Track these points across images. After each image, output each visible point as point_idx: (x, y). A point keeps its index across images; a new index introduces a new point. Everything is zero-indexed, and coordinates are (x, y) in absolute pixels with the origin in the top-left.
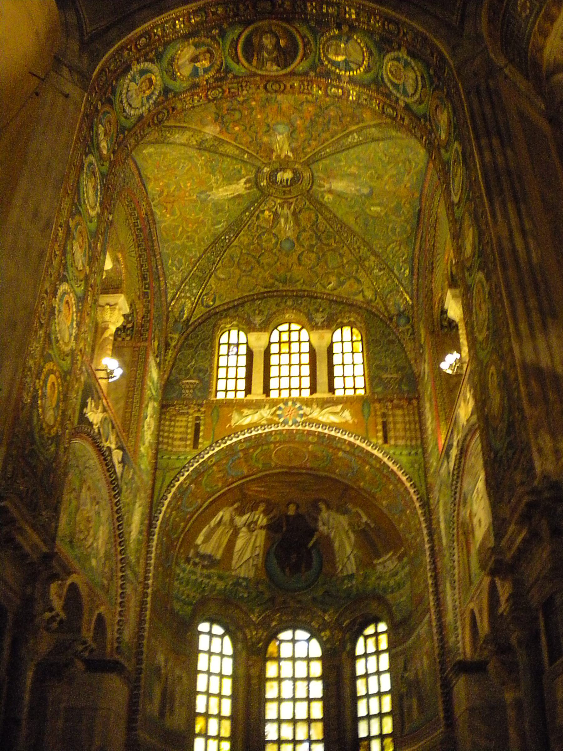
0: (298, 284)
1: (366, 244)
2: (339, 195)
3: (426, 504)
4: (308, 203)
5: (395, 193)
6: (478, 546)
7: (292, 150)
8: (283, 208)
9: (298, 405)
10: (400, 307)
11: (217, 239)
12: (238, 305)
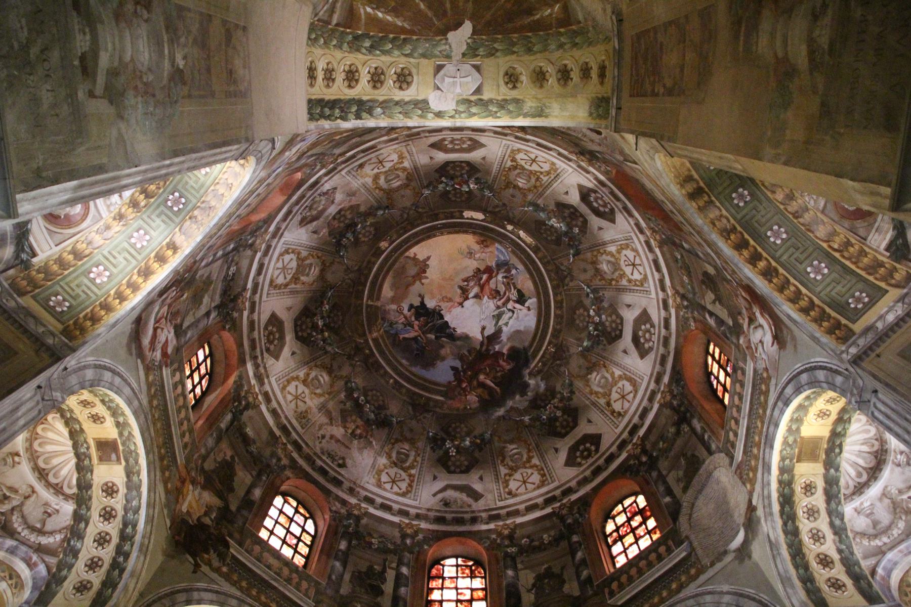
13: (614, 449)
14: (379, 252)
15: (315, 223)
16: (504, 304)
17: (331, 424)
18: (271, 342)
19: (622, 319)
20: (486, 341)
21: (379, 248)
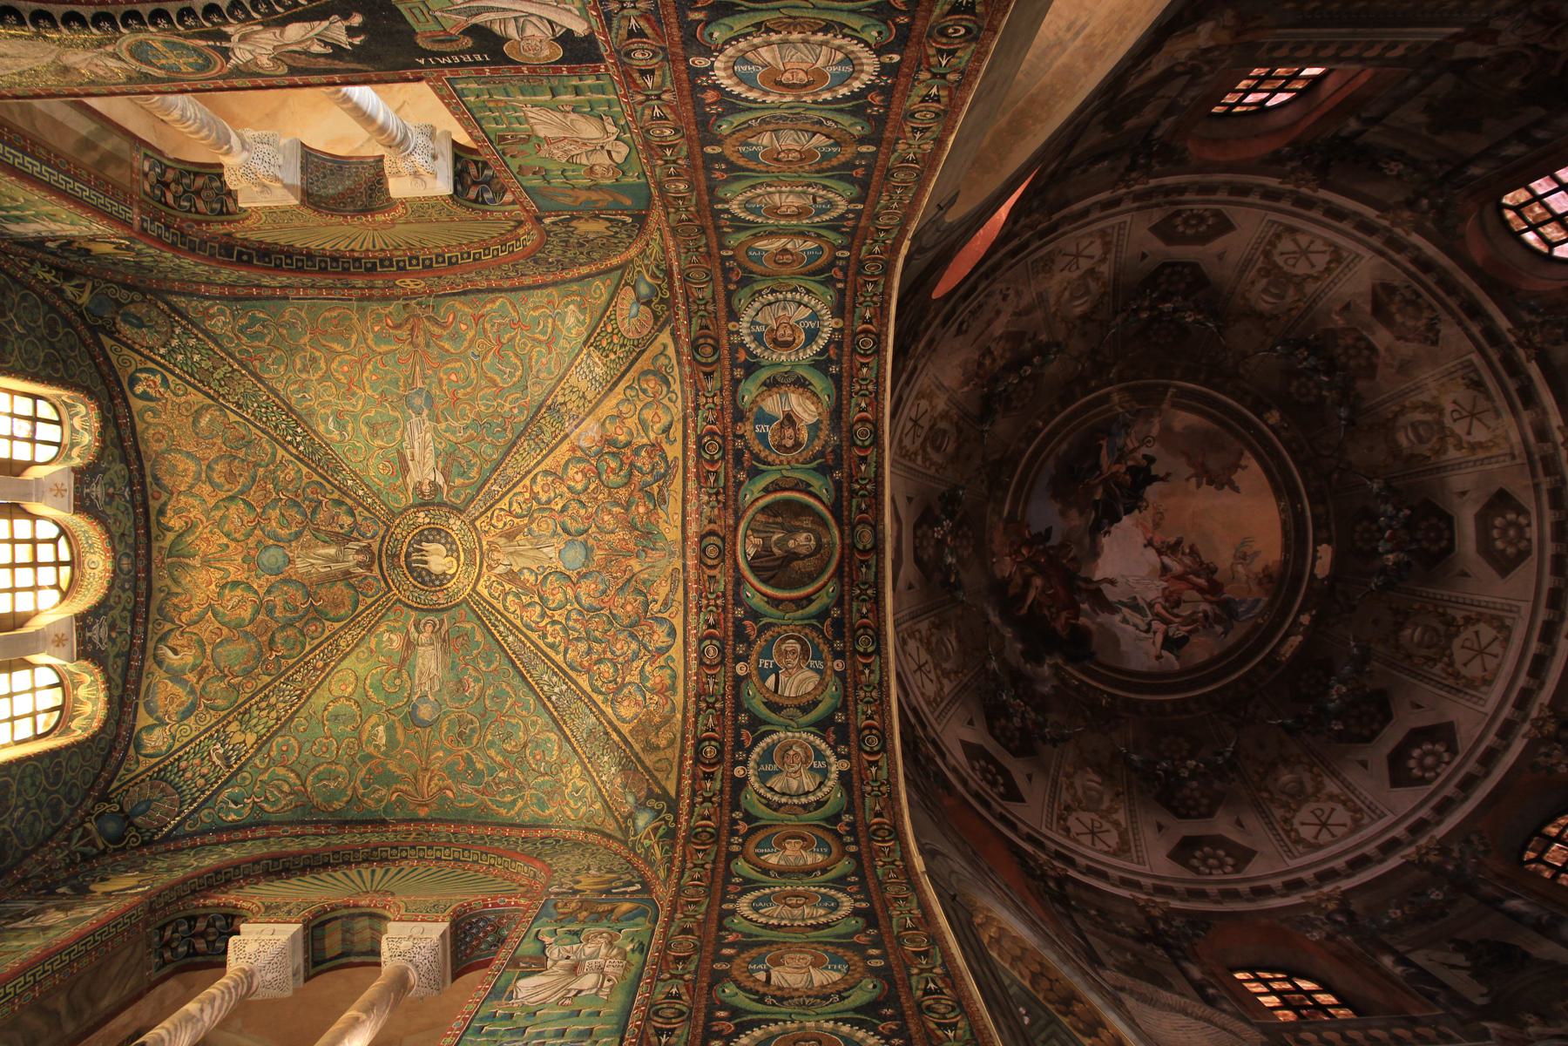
0: (169, 582)
1: (284, 725)
2: (404, 662)
4: (370, 601)
5: (426, 770)
8: (358, 552)
10: (143, 813)
11: (299, 419)
12: (123, 448)
13: (1026, 829)
14: (1260, 407)
15: (1368, 308)
16: (1157, 616)
17: (1015, 314)
18: (1186, 222)
19: (1210, 814)
20: (1092, 587)
21: (1268, 408)
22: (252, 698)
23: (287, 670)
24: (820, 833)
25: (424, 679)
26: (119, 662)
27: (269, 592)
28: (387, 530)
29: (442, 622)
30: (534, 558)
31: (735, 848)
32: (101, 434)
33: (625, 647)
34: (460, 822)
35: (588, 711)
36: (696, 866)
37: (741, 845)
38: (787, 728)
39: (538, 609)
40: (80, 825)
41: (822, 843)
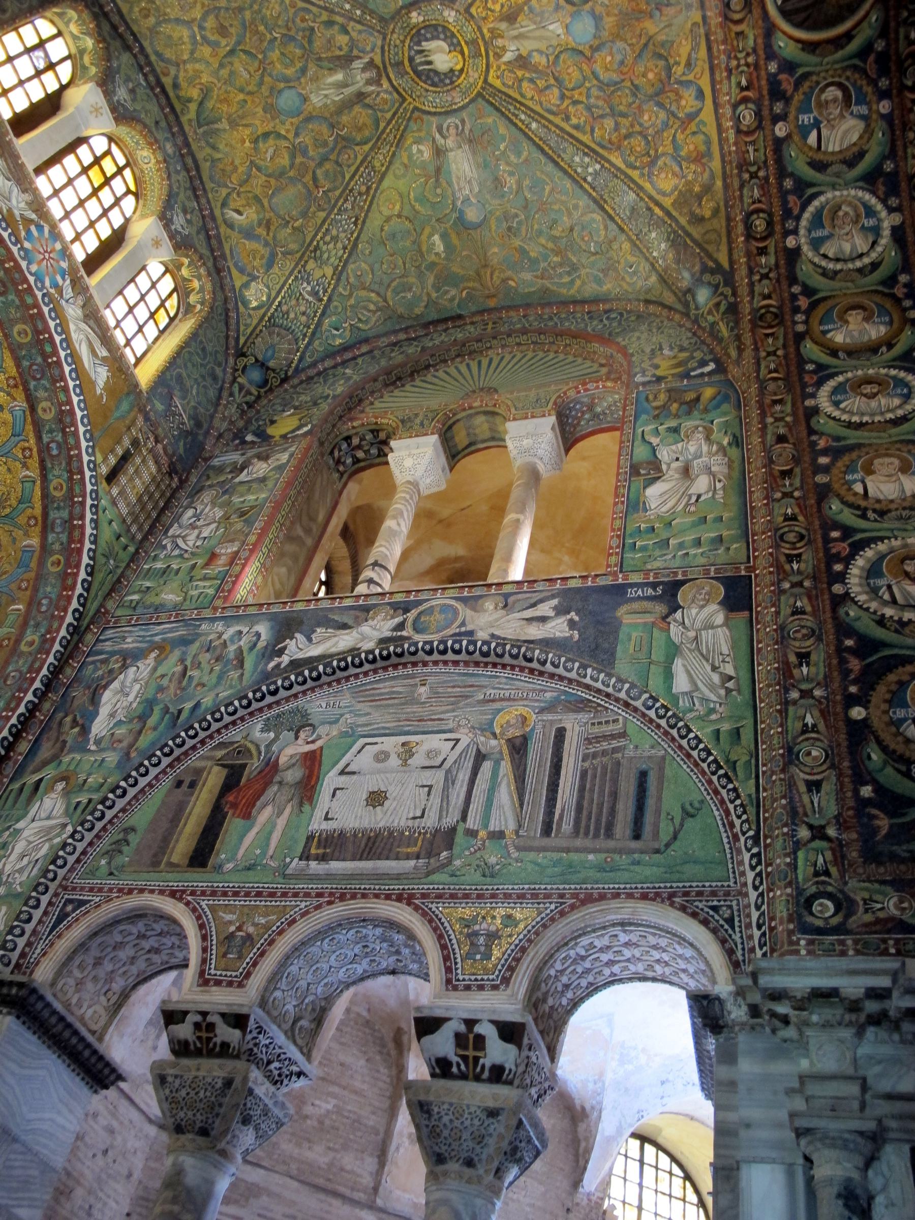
0: (208, 150)
3: (77, 631)
4: (388, 115)
5: (486, 266)
6: (317, 824)
7: (520, 57)
8: (364, 70)
9: (64, 265)
10: (272, 357)
22: (316, 235)
23: (337, 201)
24: (878, 299)
25: (462, 184)
26: (202, 236)
27: (297, 135)
28: (384, 39)
29: (463, 122)
30: (541, 38)
31: (800, 328)
32: (100, 35)
33: (652, 117)
34: (528, 306)
35: (625, 188)
36: (769, 354)
37: (806, 322)
38: (834, 187)
39: (556, 91)
40: (234, 380)
41: (883, 311)
